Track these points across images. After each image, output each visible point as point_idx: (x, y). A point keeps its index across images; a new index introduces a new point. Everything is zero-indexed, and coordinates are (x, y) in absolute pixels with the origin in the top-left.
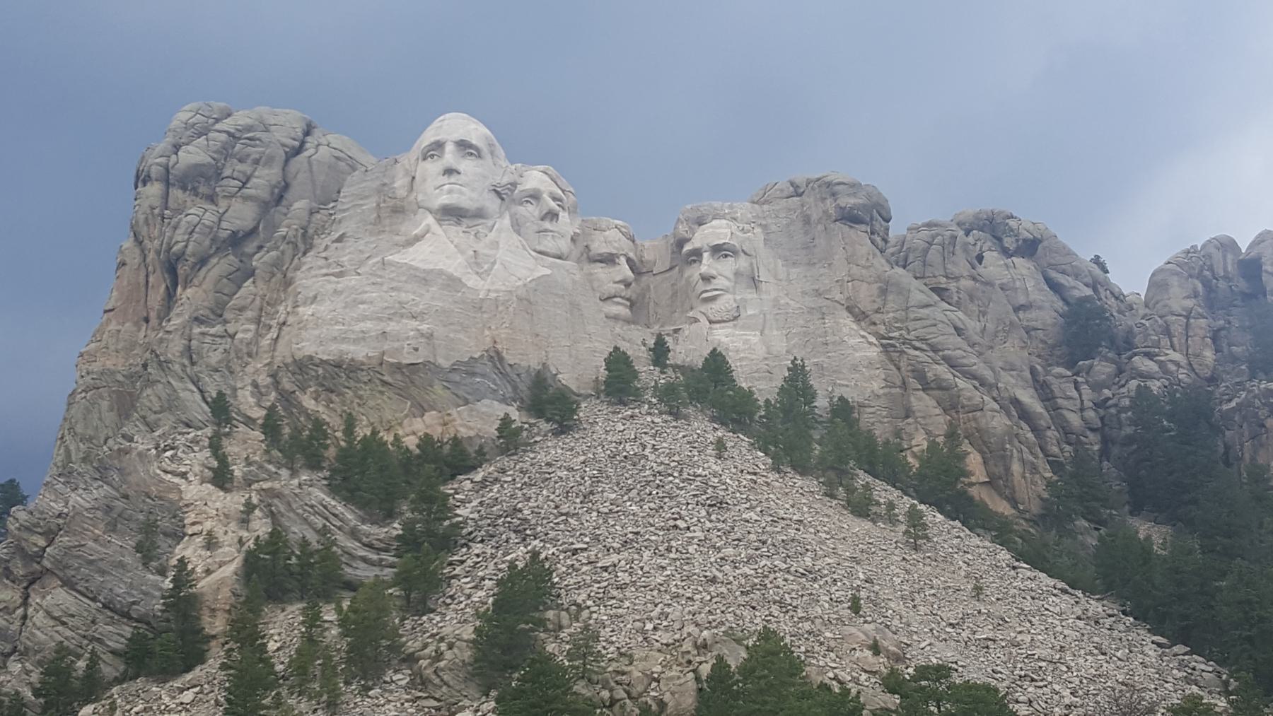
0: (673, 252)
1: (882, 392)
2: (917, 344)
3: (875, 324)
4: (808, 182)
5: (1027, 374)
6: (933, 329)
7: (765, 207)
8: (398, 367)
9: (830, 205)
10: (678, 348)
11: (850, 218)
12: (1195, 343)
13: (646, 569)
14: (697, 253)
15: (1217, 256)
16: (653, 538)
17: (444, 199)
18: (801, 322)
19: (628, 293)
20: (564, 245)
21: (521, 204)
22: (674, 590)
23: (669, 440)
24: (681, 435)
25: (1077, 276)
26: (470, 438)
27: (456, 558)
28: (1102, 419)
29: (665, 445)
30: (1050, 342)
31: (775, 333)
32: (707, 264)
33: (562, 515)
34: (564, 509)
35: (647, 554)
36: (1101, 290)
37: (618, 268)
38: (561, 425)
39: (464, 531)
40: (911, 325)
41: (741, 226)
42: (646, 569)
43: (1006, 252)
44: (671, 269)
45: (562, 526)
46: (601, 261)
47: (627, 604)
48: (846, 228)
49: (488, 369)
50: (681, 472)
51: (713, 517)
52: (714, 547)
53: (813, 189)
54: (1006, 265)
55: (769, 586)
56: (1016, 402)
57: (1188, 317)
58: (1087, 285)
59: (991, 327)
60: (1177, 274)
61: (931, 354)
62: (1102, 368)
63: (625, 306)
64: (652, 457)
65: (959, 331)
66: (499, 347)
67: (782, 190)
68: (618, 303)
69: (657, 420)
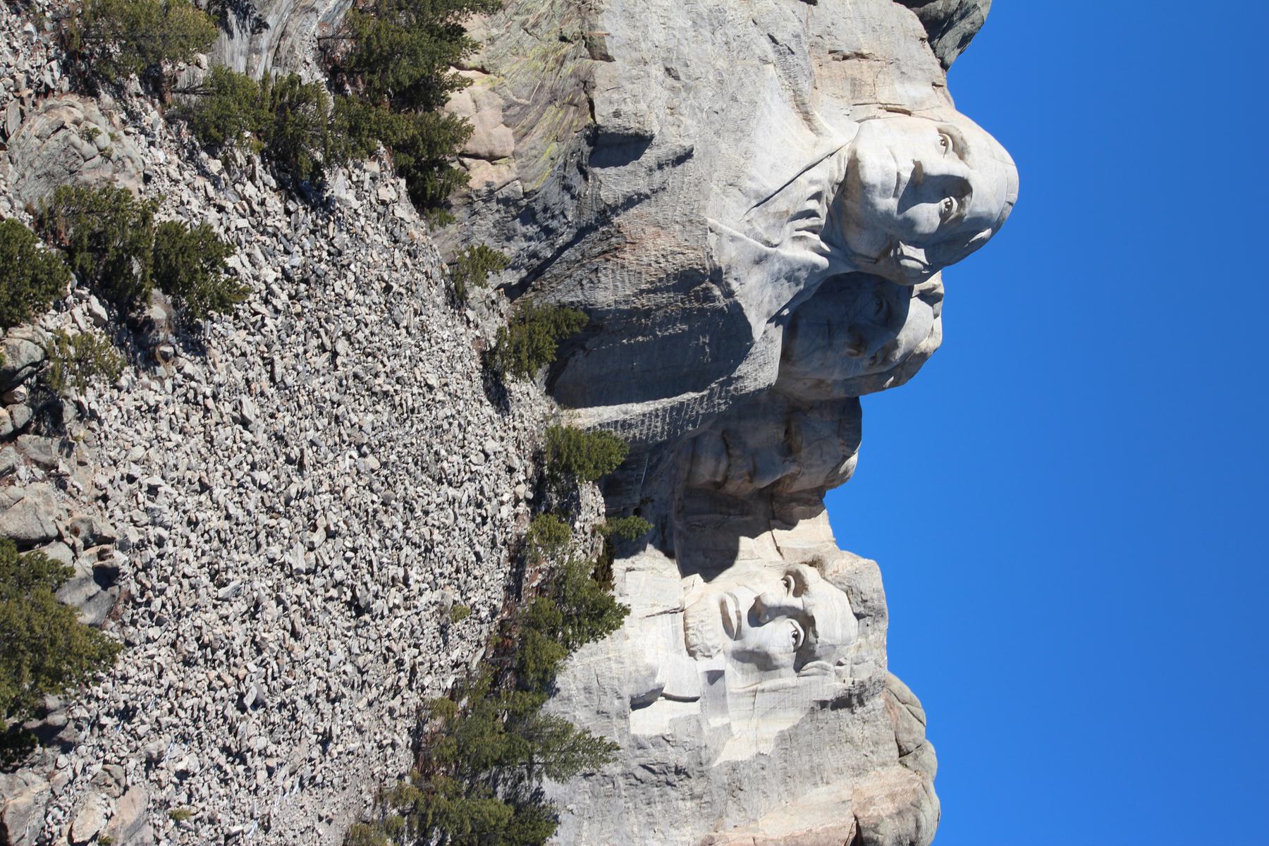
8: (586, 84)
13: (239, 474)
18: (684, 760)
24: (478, 548)
27: (259, 167)
31: (667, 717)
37: (778, 459)
38: (493, 352)
46: (786, 432)
47: (179, 438)
51: (334, 593)
55: (213, 674)
63: (715, 474)
67: (910, 731)
68: (718, 462)
69: (506, 511)
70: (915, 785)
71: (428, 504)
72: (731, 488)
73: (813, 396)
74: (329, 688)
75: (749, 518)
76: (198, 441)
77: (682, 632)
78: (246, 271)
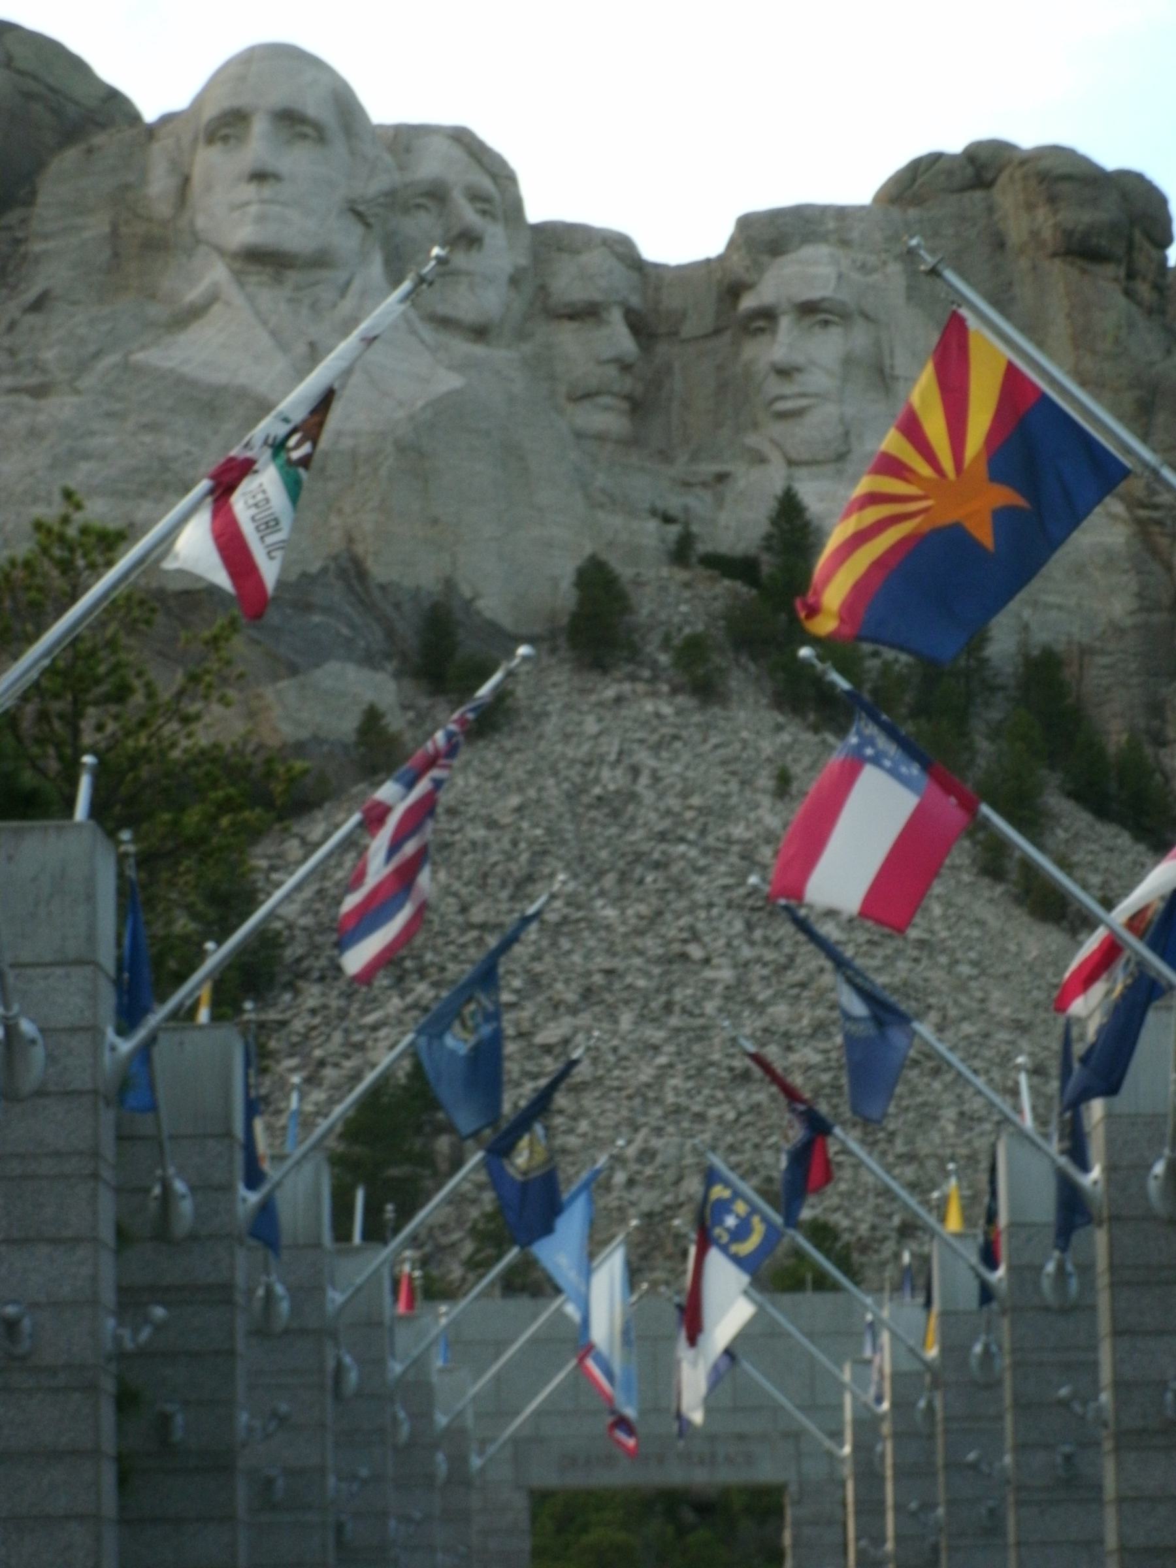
0: (720, 300)
1: (1129, 622)
7: (913, 213)
10: (723, 517)
13: (624, 1051)
14: (768, 315)
16: (641, 983)
19: (627, 384)
21: (406, 209)
22: (670, 1098)
23: (686, 757)
24: (708, 746)
29: (677, 768)
32: (783, 343)
33: (471, 926)
34: (478, 914)
35: (626, 1020)
37: (605, 331)
39: (290, 953)
41: (860, 257)
42: (624, 1051)
46: (571, 317)
47: (584, 1126)
50: (703, 832)
51: (758, 934)
52: (751, 1001)
53: (1011, 177)
64: (649, 797)
67: (950, 173)
68: (607, 408)
69: (667, 710)
70: (1018, 174)
71: (656, 810)
72: (639, 389)
74: (870, 942)
75: (677, 365)
76: (588, 1101)
77: (815, 469)
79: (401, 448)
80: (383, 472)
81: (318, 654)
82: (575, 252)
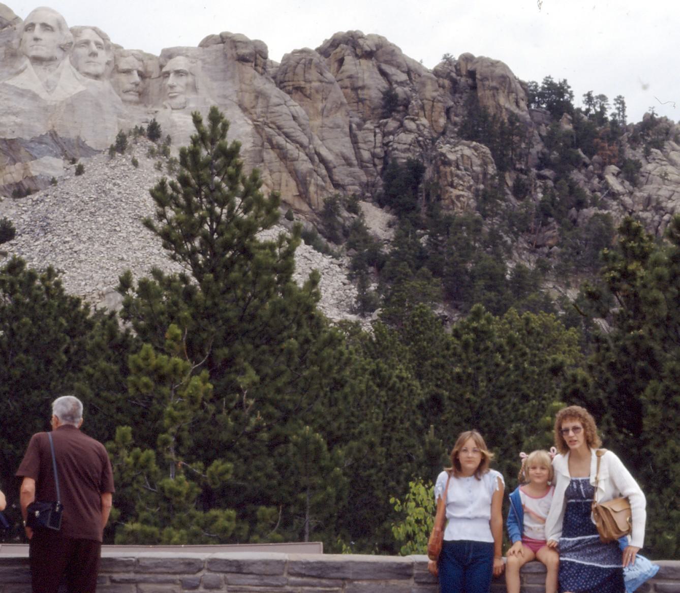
1: (250, 149)
2: (271, 125)
3: (251, 114)
4: (227, 38)
5: (347, 130)
6: (280, 118)
7: (206, 49)
9: (234, 52)
11: (243, 59)
12: (435, 114)
15: (463, 64)
17: (33, 53)
20: (100, 69)
25: (398, 67)
26: (36, 176)
28: (385, 152)
30: (372, 107)
36: (413, 75)
40: (269, 115)
43: (357, 56)
44: (159, 77)
45: (64, 228)
46: (124, 72)
48: (240, 65)
49: (49, 140)
52: (129, 242)
54: (356, 65)
56: (319, 155)
57: (433, 101)
58: (403, 72)
59: (329, 106)
60: (431, 79)
61: (277, 130)
62: (392, 124)
65: (295, 118)
66: (55, 129)
67: (215, 40)
68: (132, 95)
72: (141, 90)
73: (112, 66)
78: (39, 248)
79: (68, 105)
80: (62, 110)
81: (42, 154)
82: (125, 57)
